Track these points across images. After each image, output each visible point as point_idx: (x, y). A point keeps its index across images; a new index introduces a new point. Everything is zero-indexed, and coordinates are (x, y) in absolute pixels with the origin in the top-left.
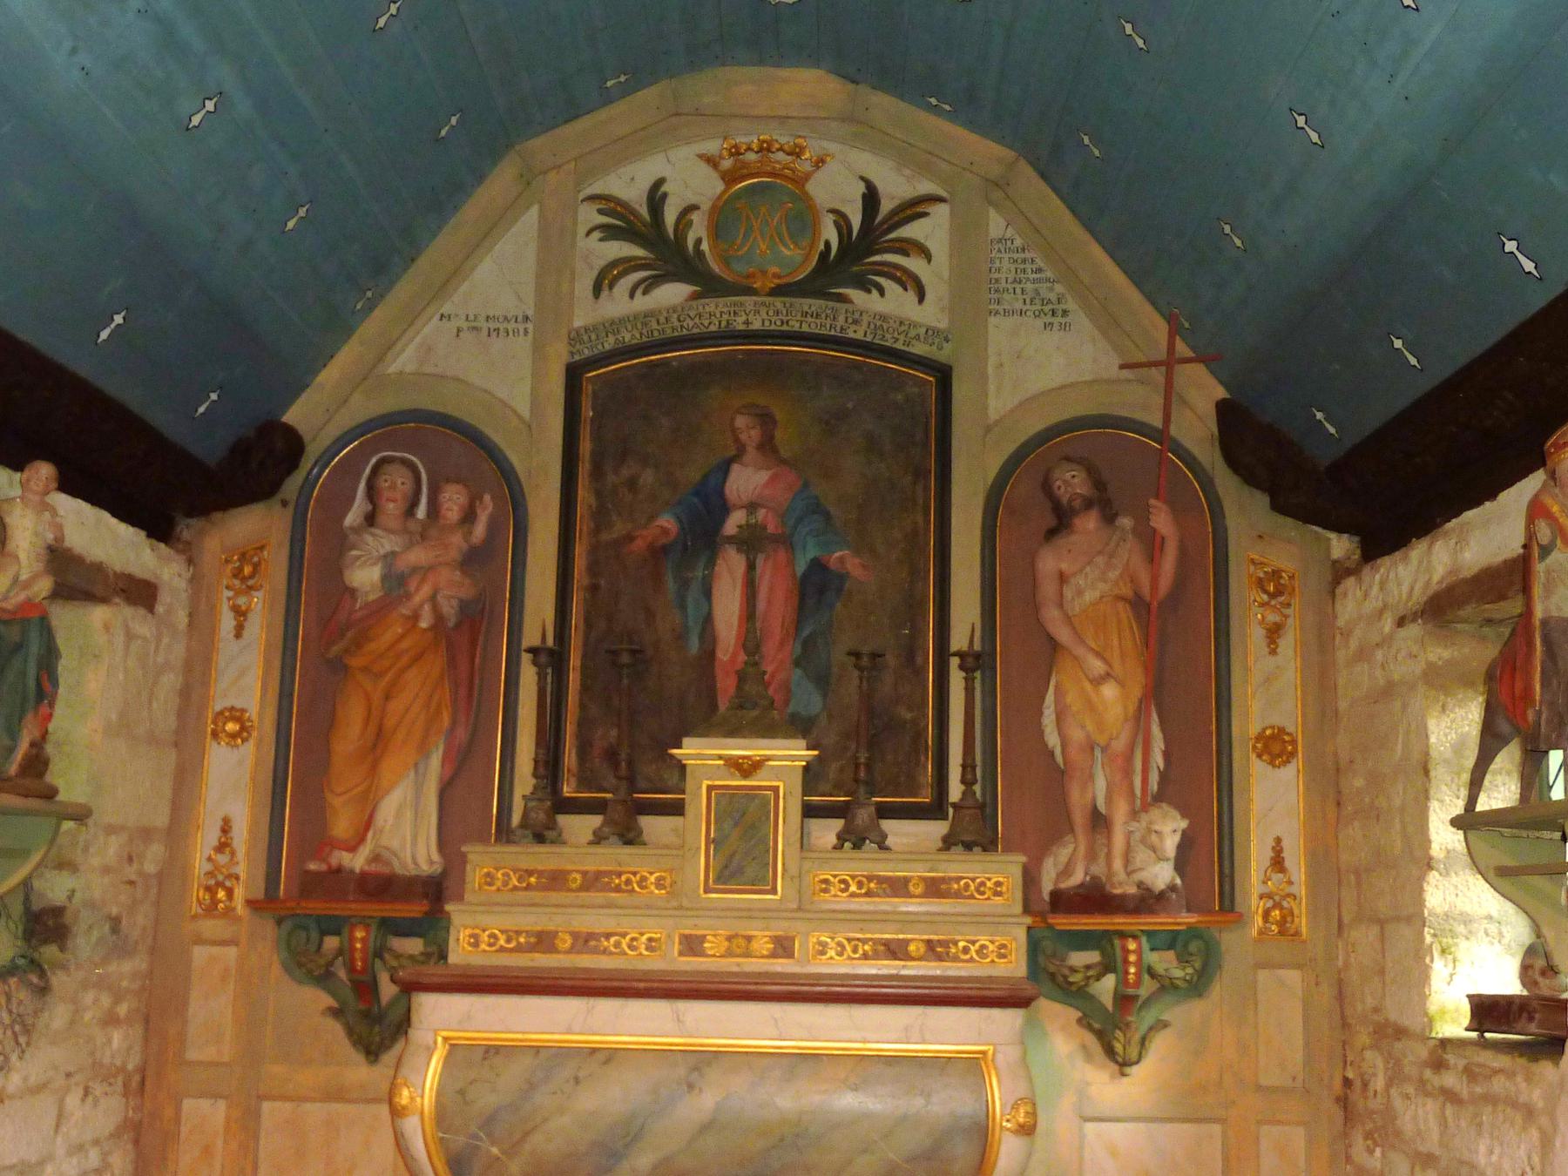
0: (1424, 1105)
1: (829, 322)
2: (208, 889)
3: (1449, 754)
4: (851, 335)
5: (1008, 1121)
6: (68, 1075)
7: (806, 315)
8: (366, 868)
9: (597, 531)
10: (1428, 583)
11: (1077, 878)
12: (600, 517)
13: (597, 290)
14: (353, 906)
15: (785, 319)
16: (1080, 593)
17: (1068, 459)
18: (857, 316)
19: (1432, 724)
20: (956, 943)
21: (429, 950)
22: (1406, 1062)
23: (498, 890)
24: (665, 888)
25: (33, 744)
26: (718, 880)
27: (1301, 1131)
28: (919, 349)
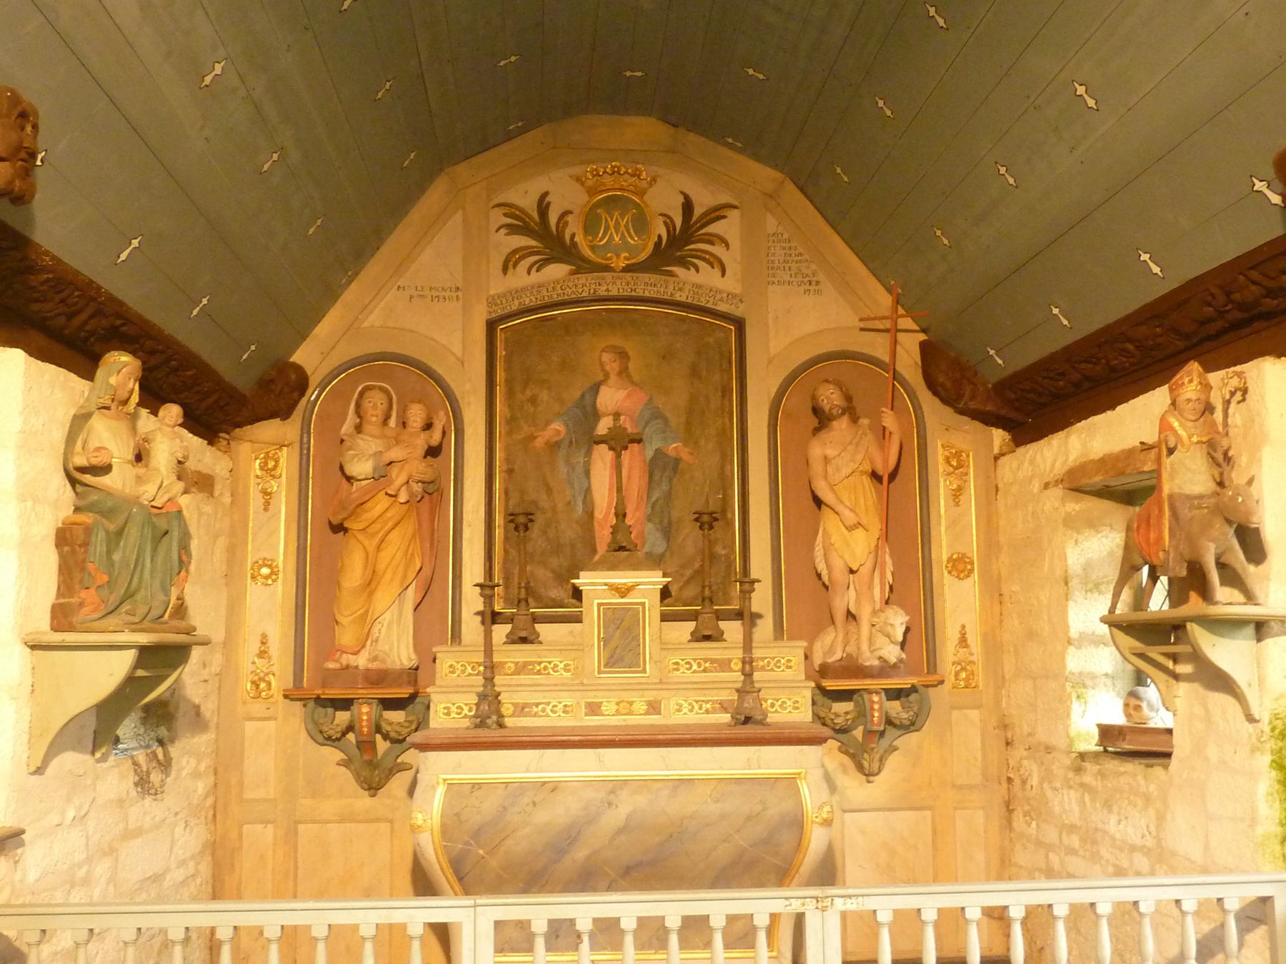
0: (1068, 795)
1: (662, 290)
2: (253, 682)
4: (679, 299)
5: (816, 817)
6: (176, 814)
7: (648, 285)
8: (370, 666)
9: (510, 433)
10: (1066, 460)
11: (838, 656)
12: (511, 421)
13: (505, 269)
15: (633, 288)
16: (838, 469)
17: (827, 381)
18: (681, 285)
20: (766, 701)
21: (410, 718)
22: (1054, 767)
23: (458, 676)
24: (569, 671)
25: (178, 599)
26: (606, 666)
27: (981, 812)
28: (723, 307)
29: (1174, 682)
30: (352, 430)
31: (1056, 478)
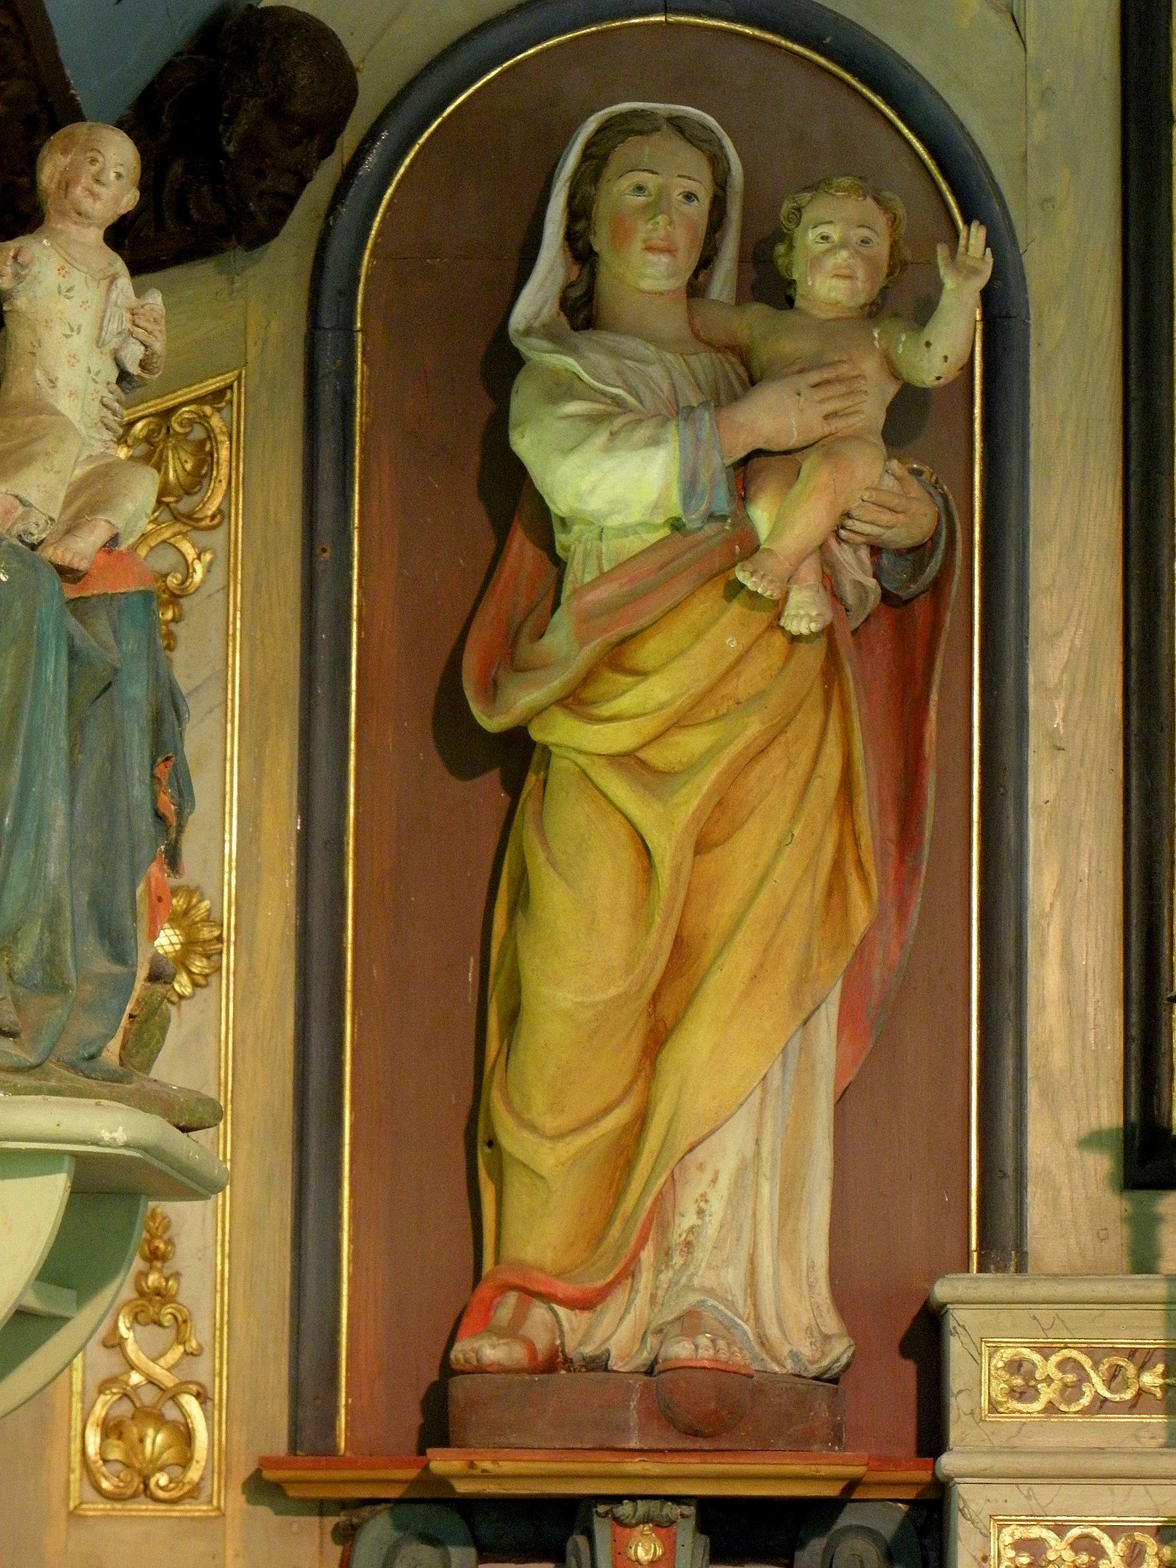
2: (111, 1429)
14: (635, 1466)
23: (1051, 1408)
30: (551, 308)
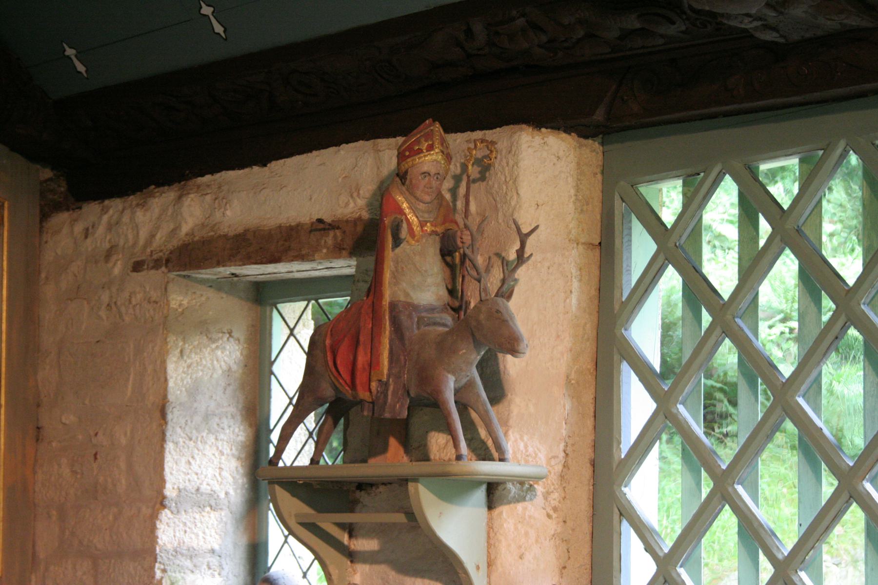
3: (184, 398)
10: (174, 231)
19: (171, 367)
29: (349, 562)
31: (155, 257)
